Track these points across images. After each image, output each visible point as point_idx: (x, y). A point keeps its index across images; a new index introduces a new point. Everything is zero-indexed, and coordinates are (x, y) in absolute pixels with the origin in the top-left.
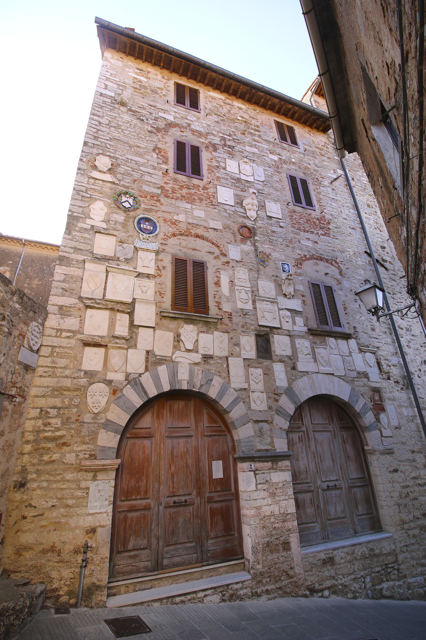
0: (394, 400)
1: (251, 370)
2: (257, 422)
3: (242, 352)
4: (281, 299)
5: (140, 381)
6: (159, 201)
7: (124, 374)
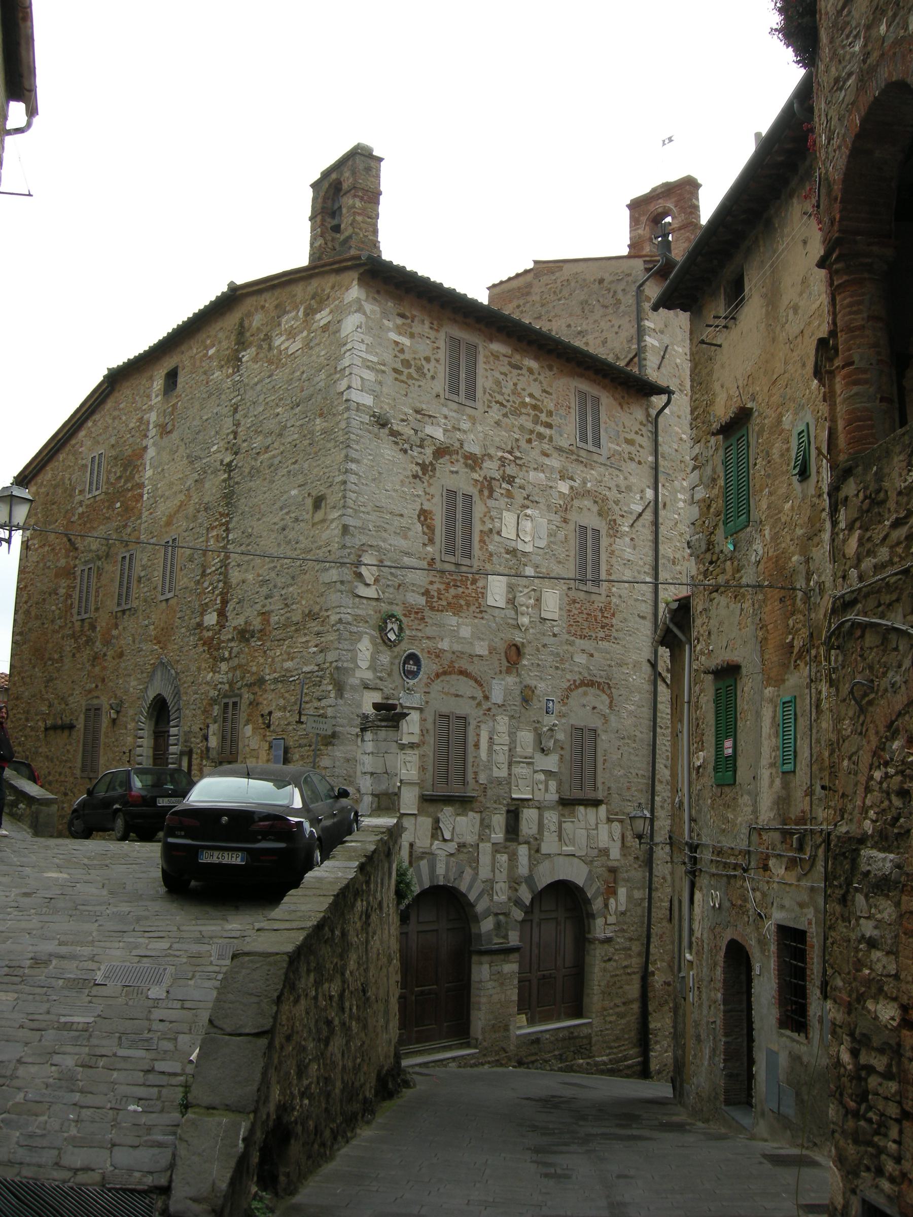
0: (627, 880)
1: (498, 856)
2: (496, 914)
4: (538, 756)
6: (423, 619)
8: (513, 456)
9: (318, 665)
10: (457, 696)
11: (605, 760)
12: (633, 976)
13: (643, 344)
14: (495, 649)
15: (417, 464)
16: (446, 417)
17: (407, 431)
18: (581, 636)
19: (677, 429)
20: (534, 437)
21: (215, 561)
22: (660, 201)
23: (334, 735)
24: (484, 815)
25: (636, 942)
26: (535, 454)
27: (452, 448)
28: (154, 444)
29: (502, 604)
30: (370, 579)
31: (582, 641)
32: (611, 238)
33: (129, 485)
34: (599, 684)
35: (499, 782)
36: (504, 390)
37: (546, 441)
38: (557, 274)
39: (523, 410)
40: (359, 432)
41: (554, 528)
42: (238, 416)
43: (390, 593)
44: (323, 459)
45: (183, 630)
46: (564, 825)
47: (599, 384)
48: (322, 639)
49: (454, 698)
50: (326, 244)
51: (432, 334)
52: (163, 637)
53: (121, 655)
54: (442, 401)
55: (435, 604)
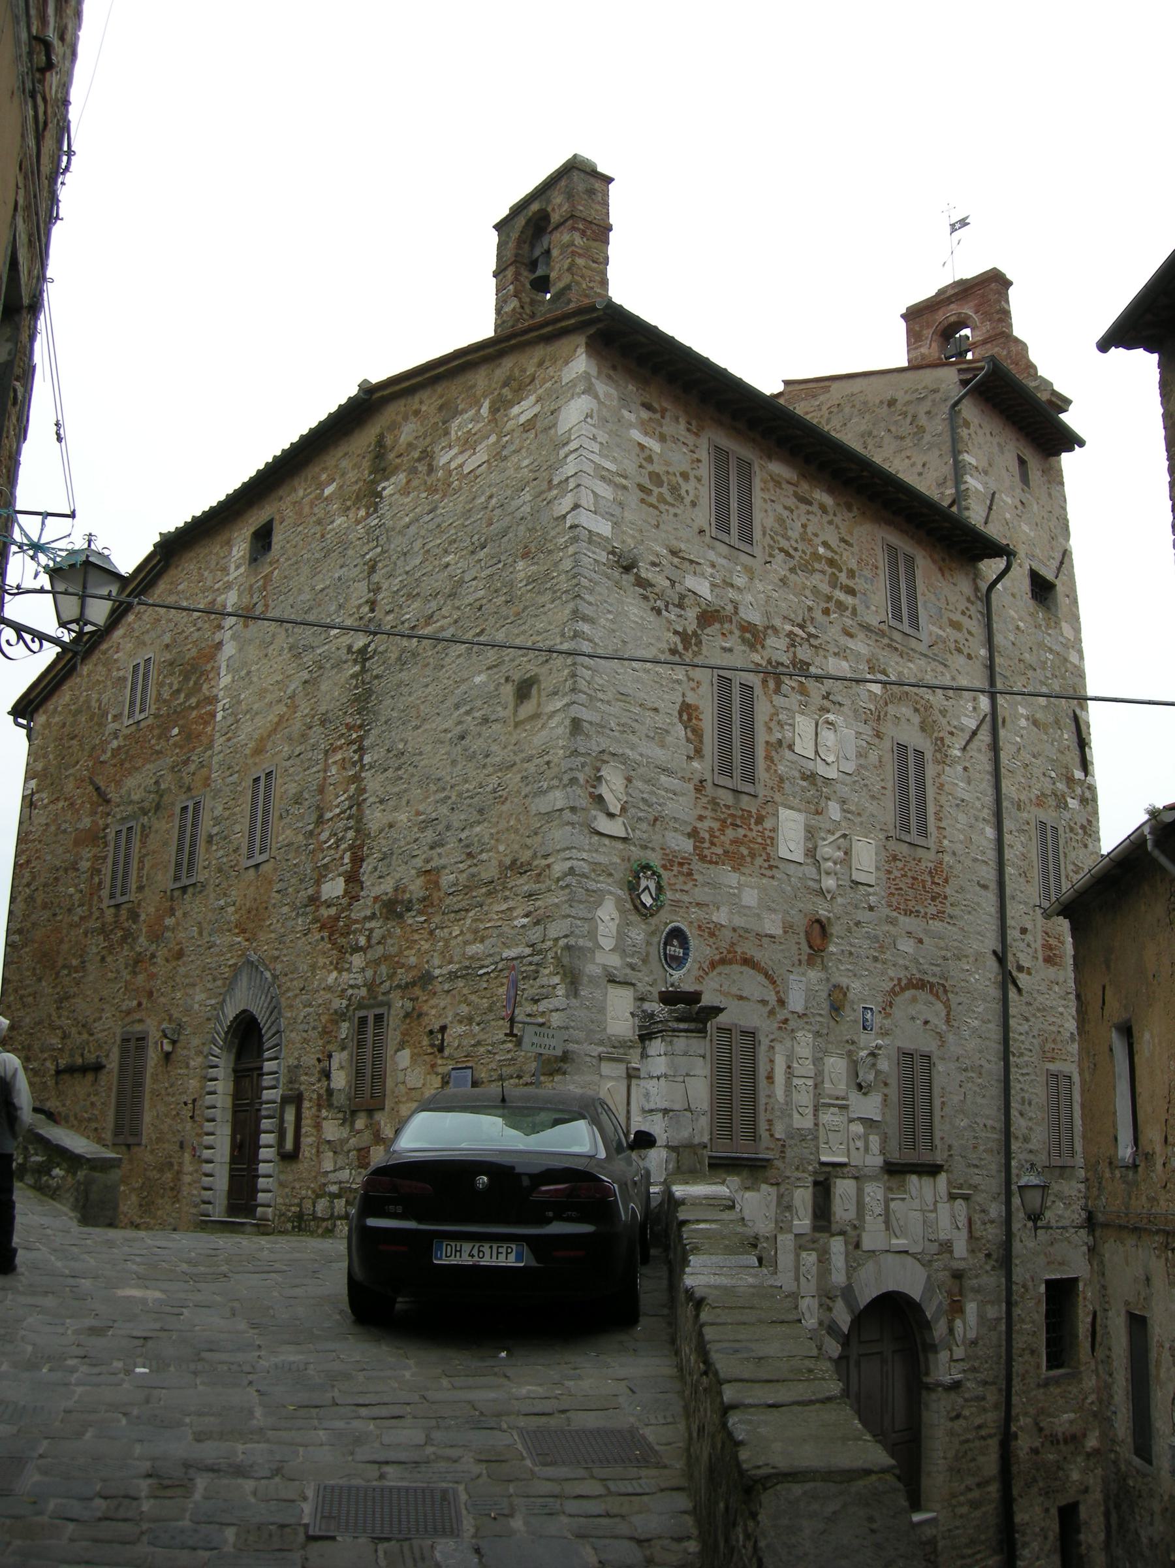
1: (804, 1254)
4: (855, 1098)
6: (690, 874)
8: (804, 633)
9: (532, 945)
10: (741, 998)
11: (943, 1103)
12: (990, 1441)
13: (963, 487)
14: (791, 927)
15: (676, 632)
16: (713, 566)
17: (661, 582)
18: (905, 910)
19: (1012, 613)
20: (832, 606)
21: (339, 800)
22: (952, 306)
23: (565, 1057)
24: (782, 1190)
25: (993, 1388)
26: (834, 632)
27: (723, 613)
28: (233, 637)
29: (799, 856)
30: (615, 808)
31: (907, 919)
32: (889, 349)
33: (193, 701)
34: (932, 985)
35: (802, 1136)
36: (790, 533)
37: (848, 613)
38: (822, 398)
39: (817, 566)
40: (594, 575)
41: (864, 744)
42: (376, 578)
43: (642, 832)
44: (530, 621)
45: (285, 909)
46: (892, 1205)
47: (912, 538)
48: (538, 903)
49: (736, 1002)
50: (522, 307)
51: (691, 439)
52: (250, 922)
53: (180, 954)
54: (707, 539)
55: (706, 852)
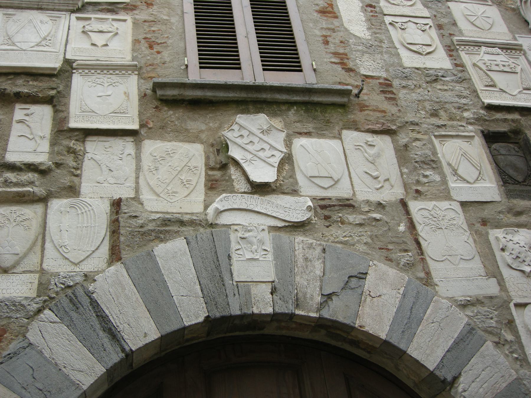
1: (496, 235)
3: (452, 185)
5: (89, 294)
7: (35, 278)
